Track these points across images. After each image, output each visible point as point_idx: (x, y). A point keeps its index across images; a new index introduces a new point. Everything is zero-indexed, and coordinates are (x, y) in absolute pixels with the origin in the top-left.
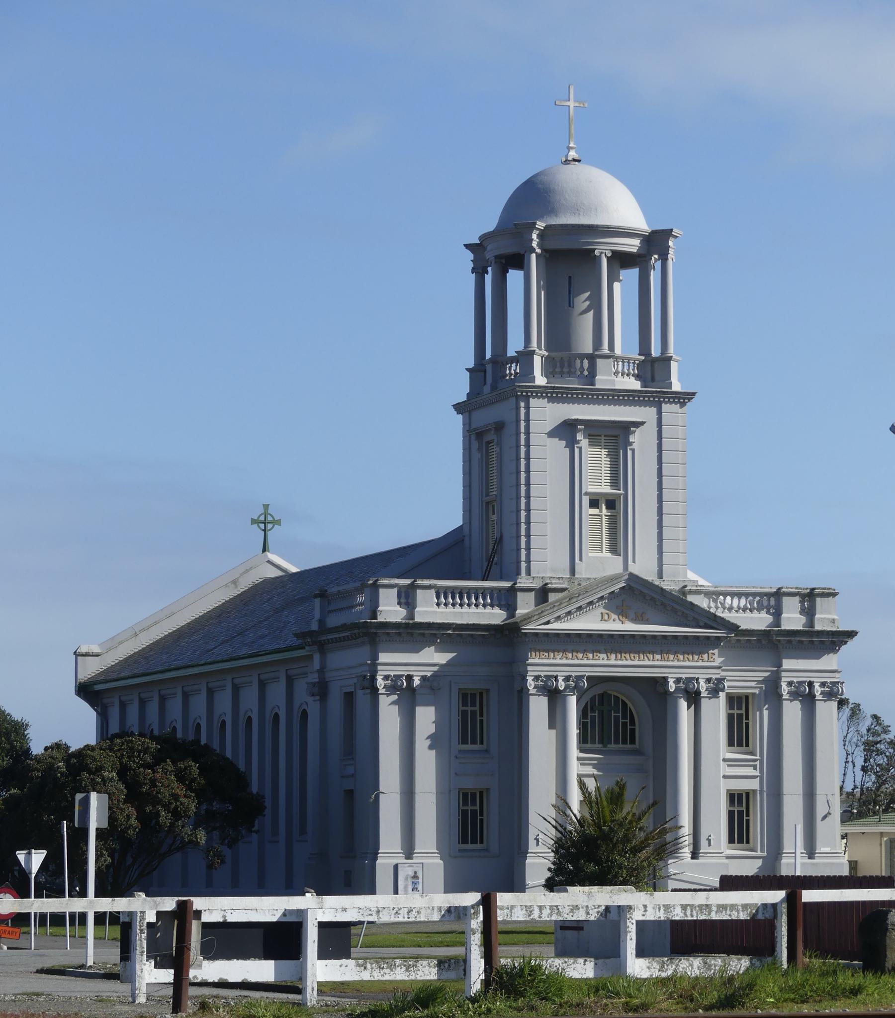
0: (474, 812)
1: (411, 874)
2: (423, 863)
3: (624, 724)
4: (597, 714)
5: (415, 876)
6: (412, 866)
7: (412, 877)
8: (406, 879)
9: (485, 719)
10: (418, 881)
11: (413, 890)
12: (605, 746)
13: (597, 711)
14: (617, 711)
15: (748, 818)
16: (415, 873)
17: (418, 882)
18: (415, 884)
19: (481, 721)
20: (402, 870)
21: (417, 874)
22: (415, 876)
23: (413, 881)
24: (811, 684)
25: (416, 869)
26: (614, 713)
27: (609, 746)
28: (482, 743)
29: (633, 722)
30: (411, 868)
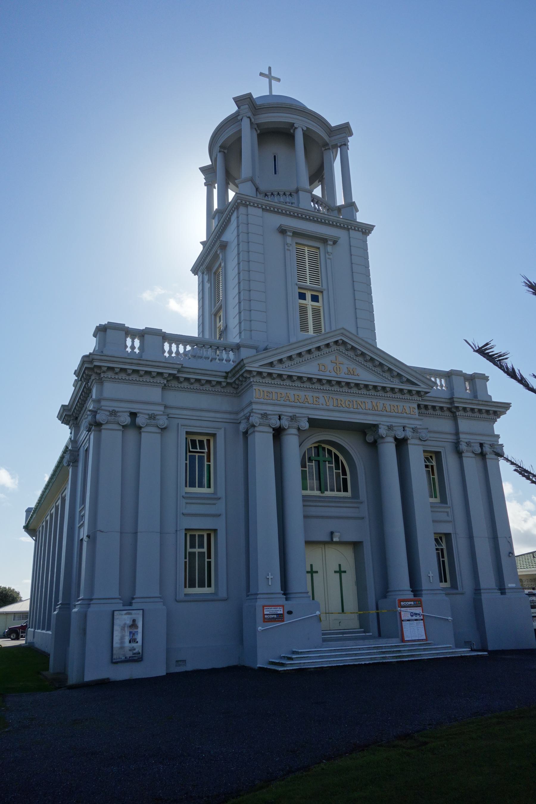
0: (201, 554)
1: (129, 622)
2: (143, 610)
3: (338, 475)
4: (314, 464)
5: (134, 625)
6: (130, 614)
7: (130, 626)
8: (123, 628)
9: (212, 463)
10: (136, 630)
11: (130, 642)
12: (322, 493)
13: (314, 461)
14: (330, 462)
15: (443, 559)
16: (134, 621)
17: (138, 631)
18: (134, 634)
19: (209, 466)
20: (117, 619)
21: (136, 622)
22: (134, 625)
23: (131, 630)
24: (481, 445)
25: (134, 616)
26: (328, 464)
27: (325, 492)
28: (209, 487)
29: (344, 473)
30: (129, 616)
